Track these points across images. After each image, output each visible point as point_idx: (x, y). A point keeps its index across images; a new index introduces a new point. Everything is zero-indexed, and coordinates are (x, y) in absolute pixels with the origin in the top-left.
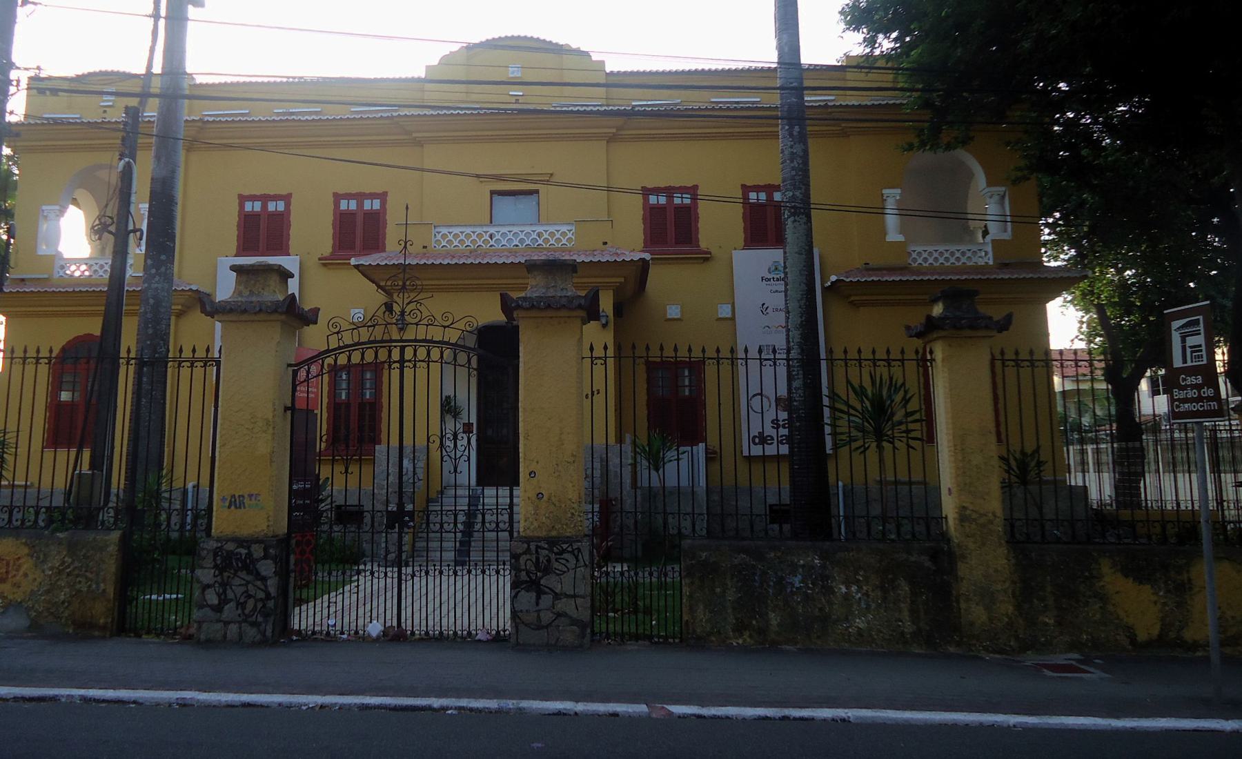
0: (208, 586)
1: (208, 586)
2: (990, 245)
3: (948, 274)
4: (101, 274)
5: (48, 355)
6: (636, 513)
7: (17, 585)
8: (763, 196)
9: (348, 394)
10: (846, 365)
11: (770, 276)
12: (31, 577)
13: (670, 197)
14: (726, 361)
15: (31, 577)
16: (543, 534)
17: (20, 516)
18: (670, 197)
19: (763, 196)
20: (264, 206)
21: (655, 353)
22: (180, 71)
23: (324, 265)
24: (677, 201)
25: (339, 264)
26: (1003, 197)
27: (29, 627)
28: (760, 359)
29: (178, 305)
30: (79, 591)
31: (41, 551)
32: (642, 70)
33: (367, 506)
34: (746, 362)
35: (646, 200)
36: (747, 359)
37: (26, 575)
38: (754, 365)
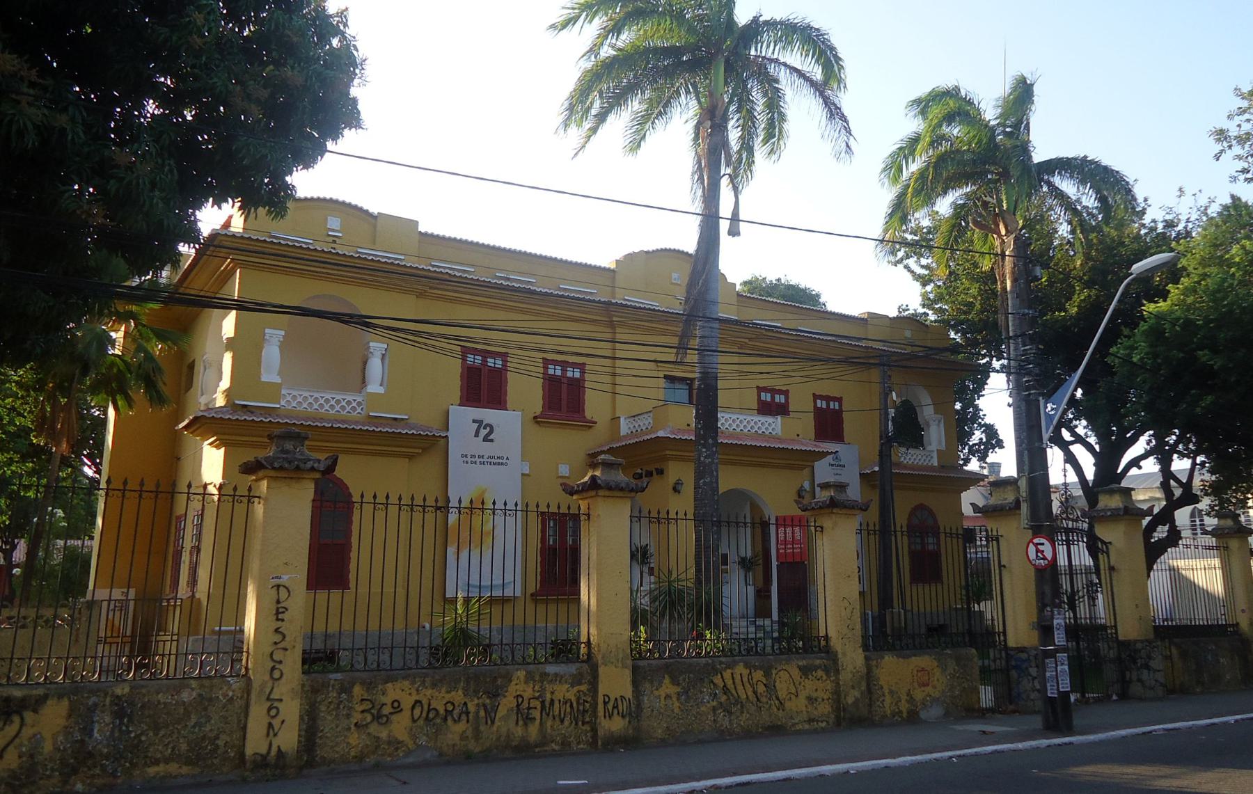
0: (1036, 678)
1: (1036, 678)
2: (936, 452)
3: (920, 470)
4: (327, 408)
5: (138, 488)
6: (546, 643)
7: (934, 687)
8: (479, 359)
9: (555, 541)
10: (424, 511)
11: (833, 463)
12: (941, 681)
13: (564, 371)
14: (431, 509)
15: (941, 681)
16: (1143, 638)
17: (762, 645)
18: (564, 371)
19: (479, 359)
20: (484, 362)
21: (543, 509)
22: (680, 277)
23: (538, 423)
24: (570, 374)
25: (581, 425)
26: (939, 421)
27: (945, 715)
28: (374, 503)
29: (419, 448)
30: (964, 688)
31: (994, 661)
32: (492, 244)
33: (496, 640)
34: (361, 506)
35: (464, 359)
36: (387, 504)
37: (938, 680)
38: (368, 509)
